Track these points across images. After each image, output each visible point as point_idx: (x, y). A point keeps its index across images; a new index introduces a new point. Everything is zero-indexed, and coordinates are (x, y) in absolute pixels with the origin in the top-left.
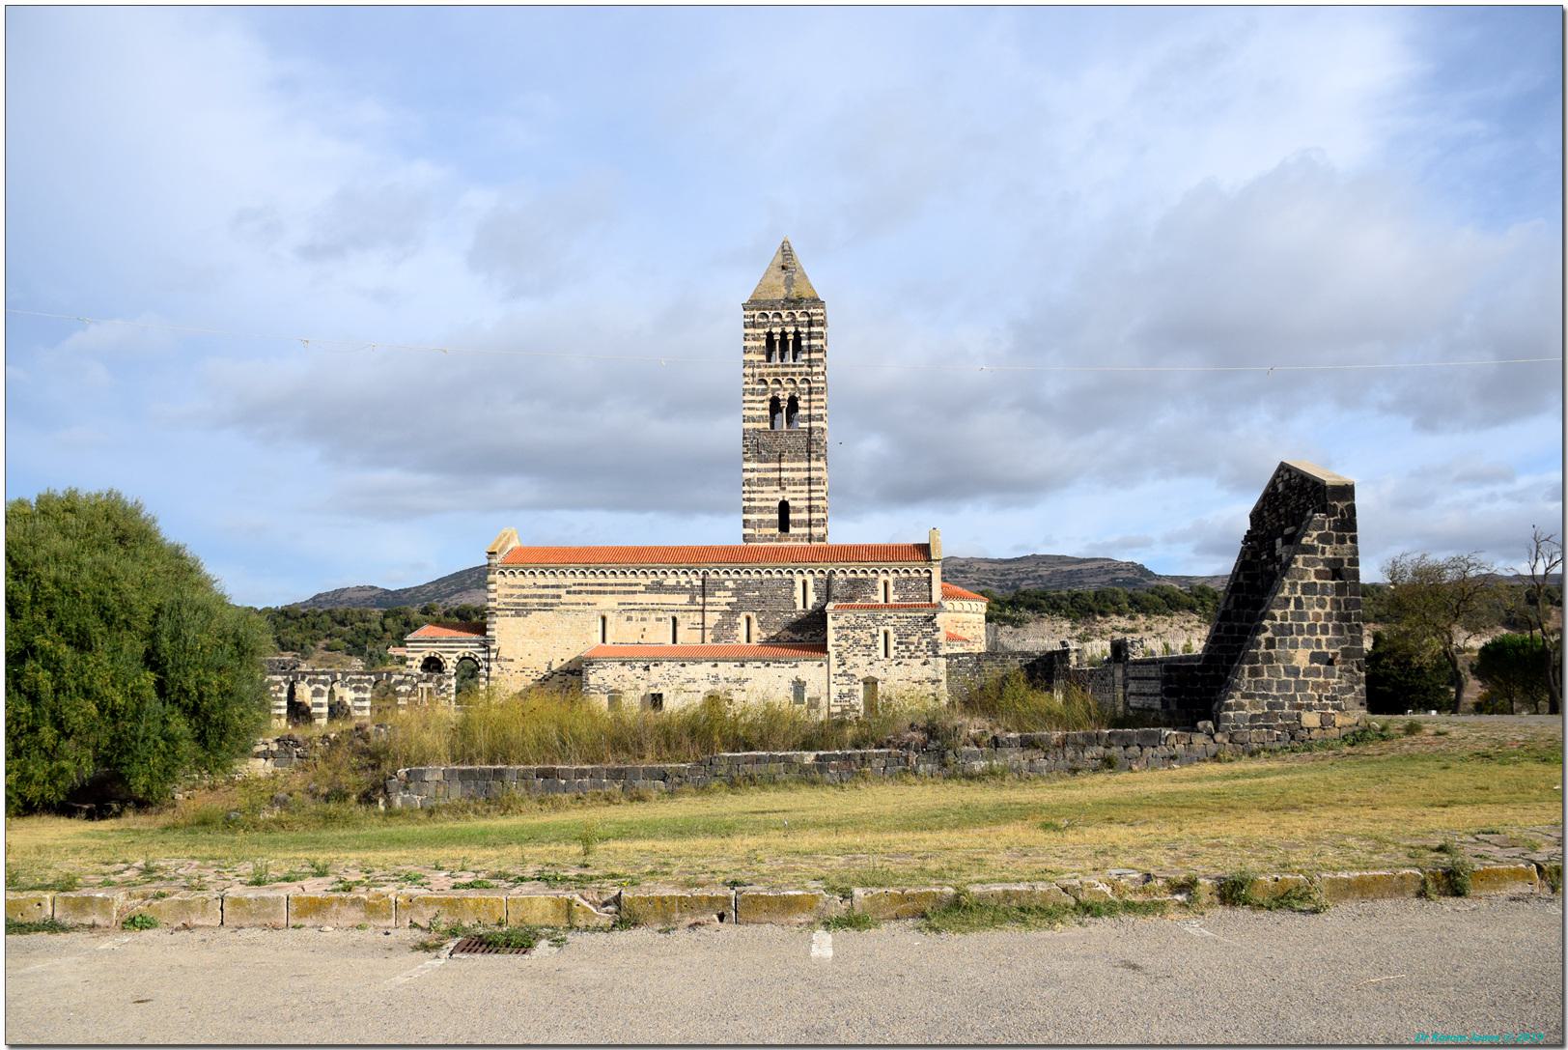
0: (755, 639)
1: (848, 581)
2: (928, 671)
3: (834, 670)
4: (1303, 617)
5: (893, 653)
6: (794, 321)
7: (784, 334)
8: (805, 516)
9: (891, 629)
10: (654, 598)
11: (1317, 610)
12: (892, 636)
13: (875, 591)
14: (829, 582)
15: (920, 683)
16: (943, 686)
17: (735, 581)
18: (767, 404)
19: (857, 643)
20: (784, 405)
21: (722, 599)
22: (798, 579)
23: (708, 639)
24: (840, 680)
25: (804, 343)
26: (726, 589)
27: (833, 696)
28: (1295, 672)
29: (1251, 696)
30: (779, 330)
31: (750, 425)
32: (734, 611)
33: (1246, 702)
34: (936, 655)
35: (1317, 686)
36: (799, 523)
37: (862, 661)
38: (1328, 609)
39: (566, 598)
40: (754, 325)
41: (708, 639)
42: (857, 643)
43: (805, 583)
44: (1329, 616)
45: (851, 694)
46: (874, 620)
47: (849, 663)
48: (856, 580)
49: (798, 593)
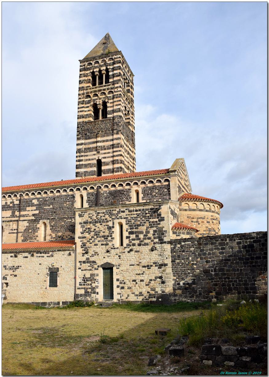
0: (48, 238)
1: (111, 193)
2: (155, 257)
5: (126, 242)
6: (106, 64)
7: (100, 71)
8: (110, 167)
9: (124, 221)
12: (125, 227)
13: (129, 198)
14: (97, 195)
15: (149, 267)
16: (169, 269)
17: (38, 199)
19: (97, 234)
21: (31, 211)
22: (77, 195)
23: (20, 239)
24: (86, 266)
25: (111, 73)
26: (33, 205)
27: (79, 280)
30: (98, 70)
31: (81, 120)
34: (162, 242)
36: (108, 171)
37: (101, 249)
40: (85, 69)
41: (20, 240)
42: (97, 234)
45: (92, 278)
46: (111, 214)
47: (91, 252)
48: (116, 192)
49: (78, 205)
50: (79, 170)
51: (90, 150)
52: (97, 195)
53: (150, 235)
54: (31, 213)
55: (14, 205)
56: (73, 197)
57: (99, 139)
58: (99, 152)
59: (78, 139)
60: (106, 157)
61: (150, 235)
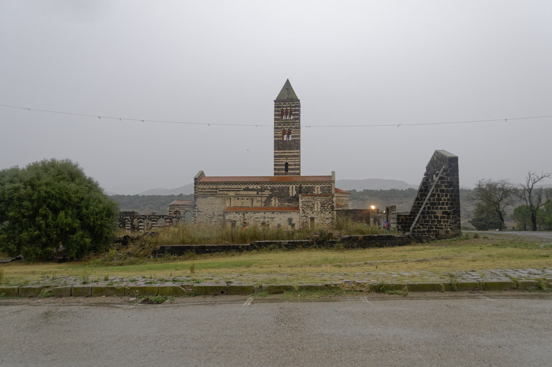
3: (301, 215)
4: (440, 200)
6: (291, 107)
7: (287, 110)
10: (246, 193)
11: (445, 197)
13: (314, 191)
14: (301, 188)
18: (281, 132)
19: (308, 206)
20: (287, 132)
22: (291, 187)
23: (263, 205)
26: (268, 190)
28: (437, 217)
29: (423, 225)
31: (276, 139)
32: (270, 197)
33: (421, 227)
35: (444, 222)
37: (310, 212)
38: (448, 197)
39: (219, 192)
43: (292, 188)
44: (448, 200)
46: (313, 199)
49: (290, 191)
50: (276, 167)
51: (282, 156)
52: (301, 188)
53: (329, 207)
54: (267, 193)
55: (258, 189)
56: (289, 188)
57: (287, 151)
58: (287, 159)
59: (275, 150)
60: (290, 161)
61: (329, 207)
